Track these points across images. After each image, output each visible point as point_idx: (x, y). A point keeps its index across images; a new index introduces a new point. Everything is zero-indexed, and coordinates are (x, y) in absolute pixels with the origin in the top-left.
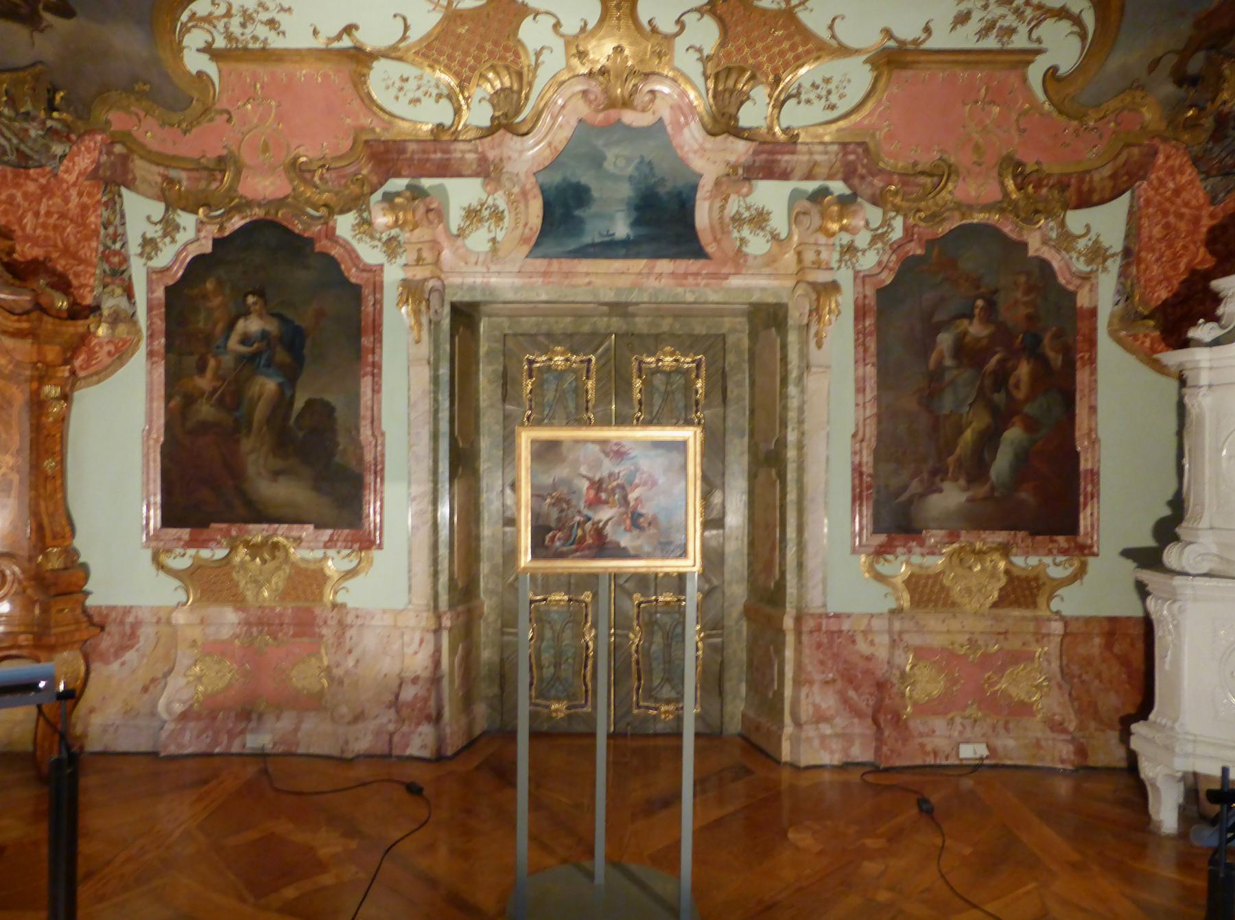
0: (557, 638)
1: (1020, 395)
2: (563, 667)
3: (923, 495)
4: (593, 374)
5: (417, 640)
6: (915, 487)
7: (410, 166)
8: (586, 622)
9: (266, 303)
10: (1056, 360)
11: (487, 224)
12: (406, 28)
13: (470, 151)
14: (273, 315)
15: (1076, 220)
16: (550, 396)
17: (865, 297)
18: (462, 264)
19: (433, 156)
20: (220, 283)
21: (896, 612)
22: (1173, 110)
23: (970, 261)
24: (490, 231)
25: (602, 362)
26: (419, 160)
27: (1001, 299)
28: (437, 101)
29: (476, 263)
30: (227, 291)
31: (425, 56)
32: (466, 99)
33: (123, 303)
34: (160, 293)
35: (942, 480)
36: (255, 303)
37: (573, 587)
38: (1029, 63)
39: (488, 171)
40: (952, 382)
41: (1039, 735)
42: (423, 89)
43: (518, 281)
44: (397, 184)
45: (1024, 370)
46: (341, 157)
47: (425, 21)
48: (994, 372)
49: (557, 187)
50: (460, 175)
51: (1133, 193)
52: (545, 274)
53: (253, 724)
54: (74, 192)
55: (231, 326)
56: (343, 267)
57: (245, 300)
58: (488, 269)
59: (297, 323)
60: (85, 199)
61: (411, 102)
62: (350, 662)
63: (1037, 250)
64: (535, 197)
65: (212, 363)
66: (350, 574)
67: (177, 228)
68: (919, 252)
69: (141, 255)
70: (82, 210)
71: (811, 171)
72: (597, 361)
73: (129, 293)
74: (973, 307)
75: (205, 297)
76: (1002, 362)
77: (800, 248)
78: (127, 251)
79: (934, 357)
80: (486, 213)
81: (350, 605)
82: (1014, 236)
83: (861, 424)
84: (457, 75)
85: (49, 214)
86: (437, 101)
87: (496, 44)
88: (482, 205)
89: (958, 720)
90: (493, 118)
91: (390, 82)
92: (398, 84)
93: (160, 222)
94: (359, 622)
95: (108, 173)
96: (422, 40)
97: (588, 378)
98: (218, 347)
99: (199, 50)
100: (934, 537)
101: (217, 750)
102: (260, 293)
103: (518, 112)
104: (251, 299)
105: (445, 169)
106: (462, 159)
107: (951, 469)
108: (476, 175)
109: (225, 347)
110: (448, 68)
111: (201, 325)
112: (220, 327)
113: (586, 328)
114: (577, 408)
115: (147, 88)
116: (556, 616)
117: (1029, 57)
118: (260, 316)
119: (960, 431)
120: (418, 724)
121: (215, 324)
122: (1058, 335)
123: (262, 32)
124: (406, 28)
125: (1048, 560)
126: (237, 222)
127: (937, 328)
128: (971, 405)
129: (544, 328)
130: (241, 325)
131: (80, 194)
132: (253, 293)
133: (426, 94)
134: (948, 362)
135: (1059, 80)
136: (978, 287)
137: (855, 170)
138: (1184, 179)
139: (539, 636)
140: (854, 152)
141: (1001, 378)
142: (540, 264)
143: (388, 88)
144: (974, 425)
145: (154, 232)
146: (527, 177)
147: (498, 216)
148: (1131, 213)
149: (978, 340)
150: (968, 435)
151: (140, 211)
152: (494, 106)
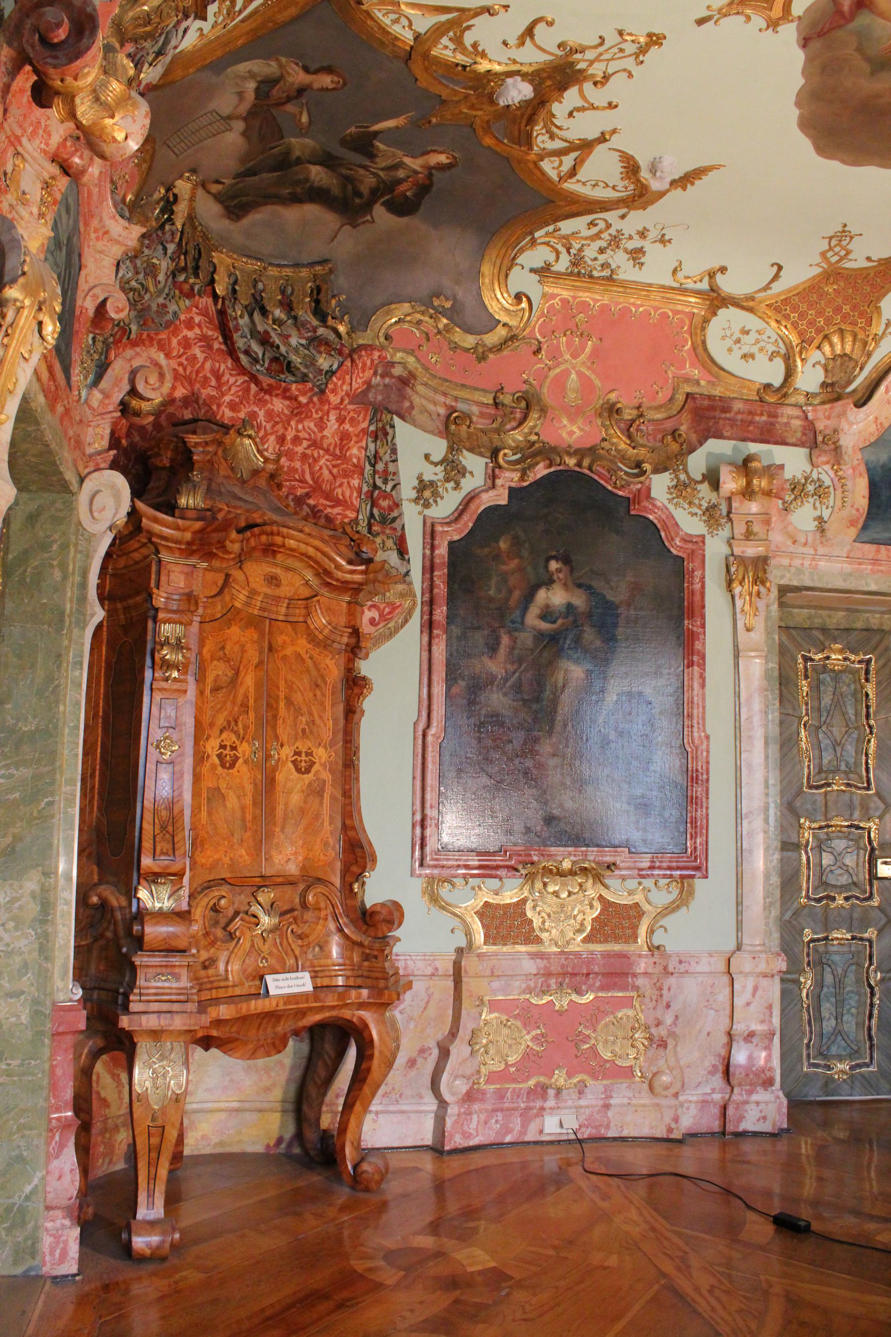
0: (839, 984)
2: (845, 1018)
4: (872, 675)
5: (750, 989)
7: (732, 427)
8: (871, 964)
9: (572, 570)
11: (811, 500)
12: (776, 277)
13: (797, 417)
14: (579, 586)
16: (827, 700)
18: (789, 543)
19: (757, 418)
20: (517, 543)
24: (815, 508)
25: (881, 663)
26: (742, 421)
28: (771, 360)
29: (805, 544)
30: (525, 553)
31: (777, 310)
32: (802, 360)
33: (393, 558)
34: (442, 551)
36: (559, 571)
37: (855, 923)
39: (814, 441)
42: (762, 344)
43: (847, 567)
44: (718, 447)
46: (658, 408)
47: (800, 272)
49: (883, 466)
50: (784, 443)
52: (875, 561)
53: (551, 1103)
54: (333, 417)
55: (529, 597)
56: (663, 534)
57: (546, 567)
58: (816, 550)
59: (609, 597)
60: (347, 426)
61: (744, 356)
62: (669, 1020)
64: (861, 475)
65: (505, 640)
66: (671, 909)
67: (463, 472)
69: (416, 500)
70: (341, 440)
72: (876, 662)
73: (402, 551)
75: (497, 557)
78: (399, 494)
80: (810, 488)
81: (669, 948)
84: (800, 334)
85: (297, 440)
86: (771, 360)
87: (854, 308)
88: (806, 479)
90: (824, 385)
91: (728, 333)
92: (737, 335)
93: (441, 463)
94: (682, 968)
95: (380, 398)
96: (779, 294)
97: (867, 680)
98: (513, 622)
99: (532, 270)
101: (508, 1139)
102: (566, 560)
103: (849, 383)
104: (554, 565)
105: (769, 435)
106: (787, 424)
108: (802, 444)
109: (522, 623)
110: (795, 325)
111: (492, 592)
112: (517, 594)
113: (859, 625)
114: (856, 714)
115: (448, 305)
116: (836, 958)
118: (565, 585)
120: (750, 1093)
121: (510, 592)
123: (619, 259)
124: (776, 277)
126: (541, 471)
129: (817, 622)
130: (542, 595)
131: (341, 420)
132: (555, 558)
133: (761, 350)
139: (819, 983)
142: (869, 549)
143: (723, 338)
145: (434, 473)
146: (854, 452)
147: (821, 492)
151: (416, 449)
152: (826, 371)
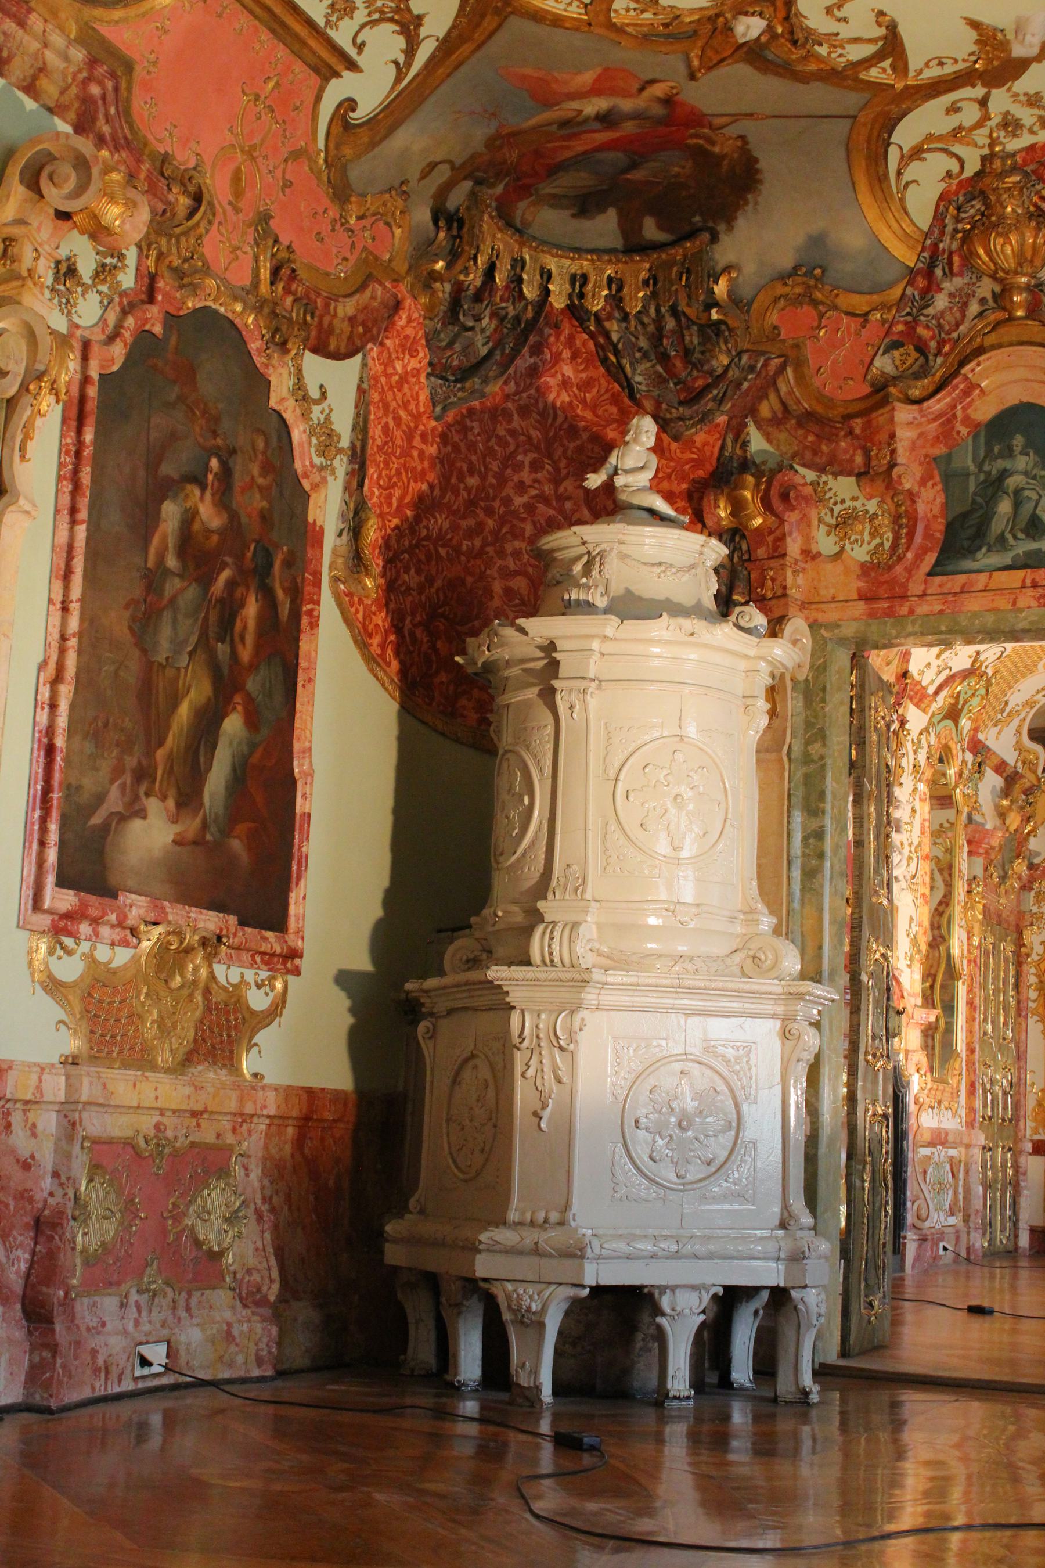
1: (245, 655)
3: (123, 818)
6: (114, 801)
10: (284, 611)
15: (317, 369)
17: (86, 380)
21: (72, 1061)
22: (424, 250)
23: (211, 383)
27: (238, 465)
35: (147, 795)
38: (337, 75)
40: (173, 600)
41: (228, 1315)
45: (251, 610)
48: (221, 601)
51: (364, 355)
63: (283, 400)
68: (158, 329)
71: (35, 78)
74: (207, 468)
76: (231, 584)
77: (16, 231)
79: (156, 541)
82: (259, 360)
83: (55, 645)
89: (134, 1296)
100: (136, 906)
107: (159, 773)
117: (339, 67)
119: (174, 704)
122: (288, 563)
125: (250, 975)
127: (164, 489)
128: (191, 654)
134: (172, 562)
135: (347, 126)
136: (215, 434)
137: (94, 119)
138: (414, 364)
140: (100, 83)
141: (228, 611)
144: (192, 693)
148: (361, 391)
149: (208, 532)
150: (184, 711)
